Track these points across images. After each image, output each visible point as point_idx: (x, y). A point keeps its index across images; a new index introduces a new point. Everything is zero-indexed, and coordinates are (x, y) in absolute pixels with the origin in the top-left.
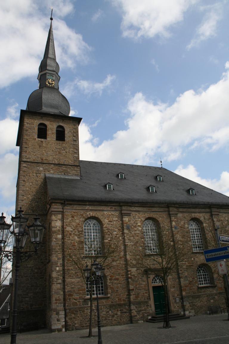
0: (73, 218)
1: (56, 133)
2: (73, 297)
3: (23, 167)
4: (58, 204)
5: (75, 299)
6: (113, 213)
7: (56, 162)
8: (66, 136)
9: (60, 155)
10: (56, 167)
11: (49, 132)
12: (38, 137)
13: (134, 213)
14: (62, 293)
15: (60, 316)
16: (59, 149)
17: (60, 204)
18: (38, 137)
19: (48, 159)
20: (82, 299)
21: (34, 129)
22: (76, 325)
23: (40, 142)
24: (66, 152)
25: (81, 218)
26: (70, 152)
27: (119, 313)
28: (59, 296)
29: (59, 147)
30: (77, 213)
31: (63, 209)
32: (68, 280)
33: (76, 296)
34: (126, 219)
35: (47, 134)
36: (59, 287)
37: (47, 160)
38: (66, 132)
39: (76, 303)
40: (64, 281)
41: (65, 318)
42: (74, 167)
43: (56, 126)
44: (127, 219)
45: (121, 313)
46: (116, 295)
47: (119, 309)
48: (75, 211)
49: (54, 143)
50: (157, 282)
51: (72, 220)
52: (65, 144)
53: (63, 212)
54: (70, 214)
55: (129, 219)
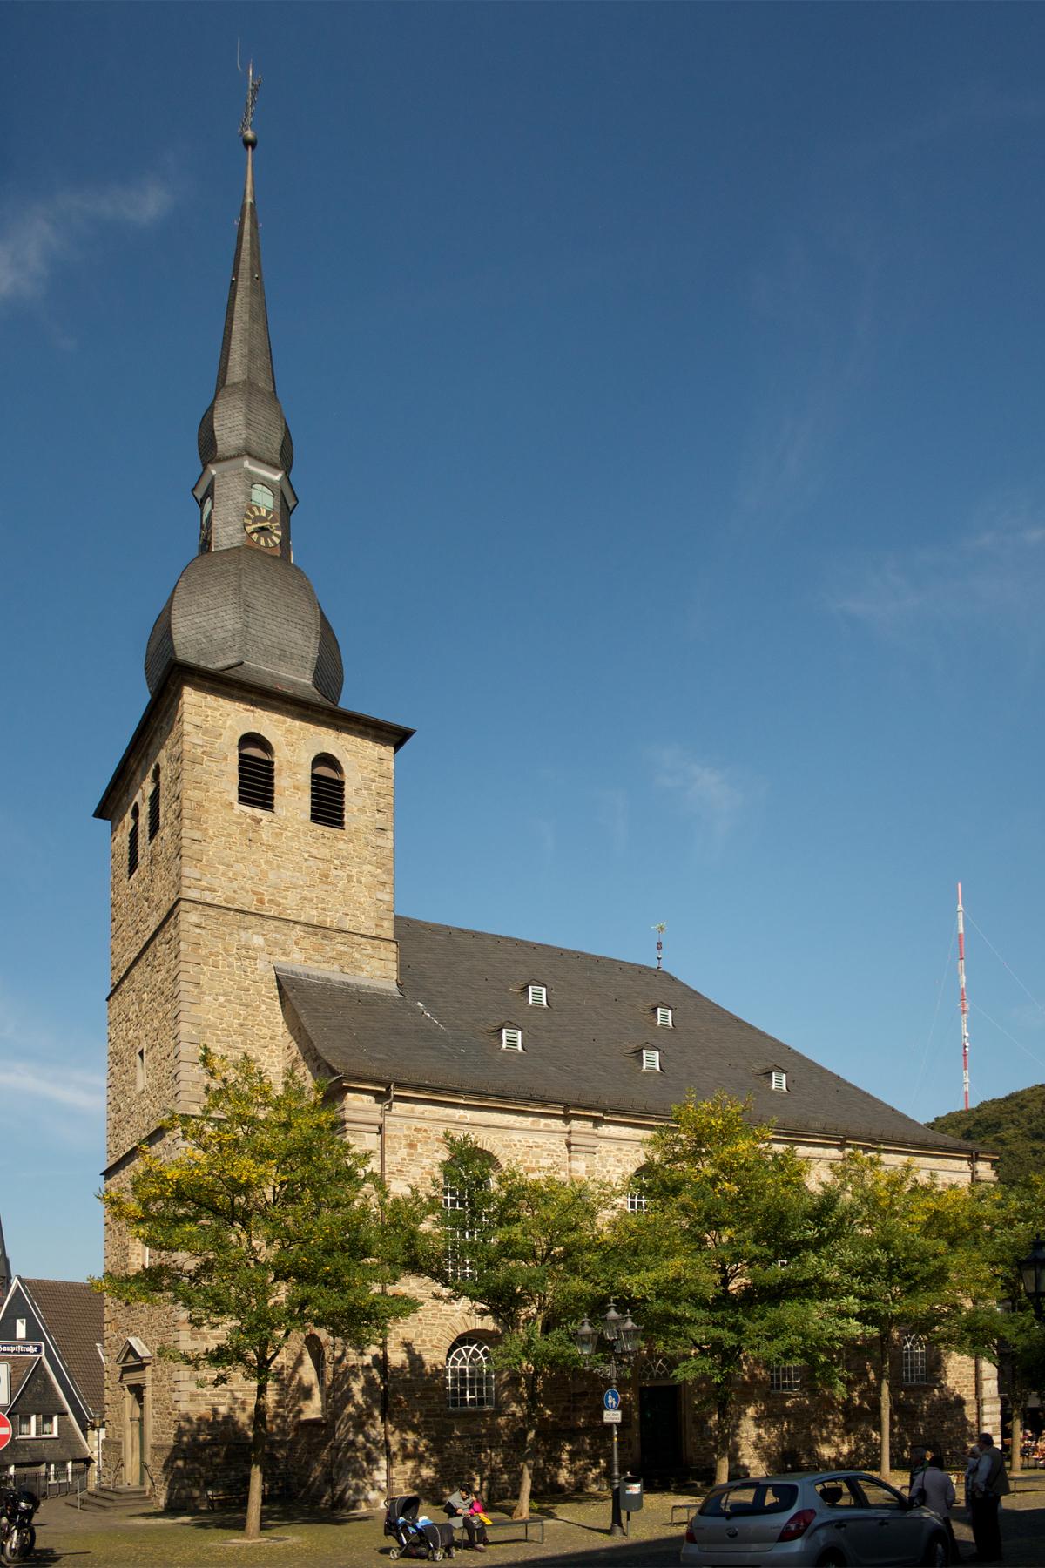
0: (412, 1151)
1: (313, 789)
3: (191, 924)
4: (365, 1097)
6: (540, 1139)
7: (309, 914)
8: (347, 805)
9: (325, 887)
10: (314, 938)
11: (281, 782)
12: (242, 800)
13: (604, 1145)
16: (322, 860)
17: (372, 1098)
18: (242, 800)
19: (282, 901)
21: (225, 759)
23: (249, 821)
24: (349, 877)
25: (437, 1151)
26: (363, 880)
29: (325, 853)
30: (425, 1131)
31: (382, 1114)
35: (276, 789)
37: (279, 905)
38: (349, 790)
42: (377, 942)
48: (419, 1127)
49: (305, 834)
51: (408, 1155)
52: (346, 842)
53: (381, 1127)
54: (405, 1136)
55: (587, 1167)
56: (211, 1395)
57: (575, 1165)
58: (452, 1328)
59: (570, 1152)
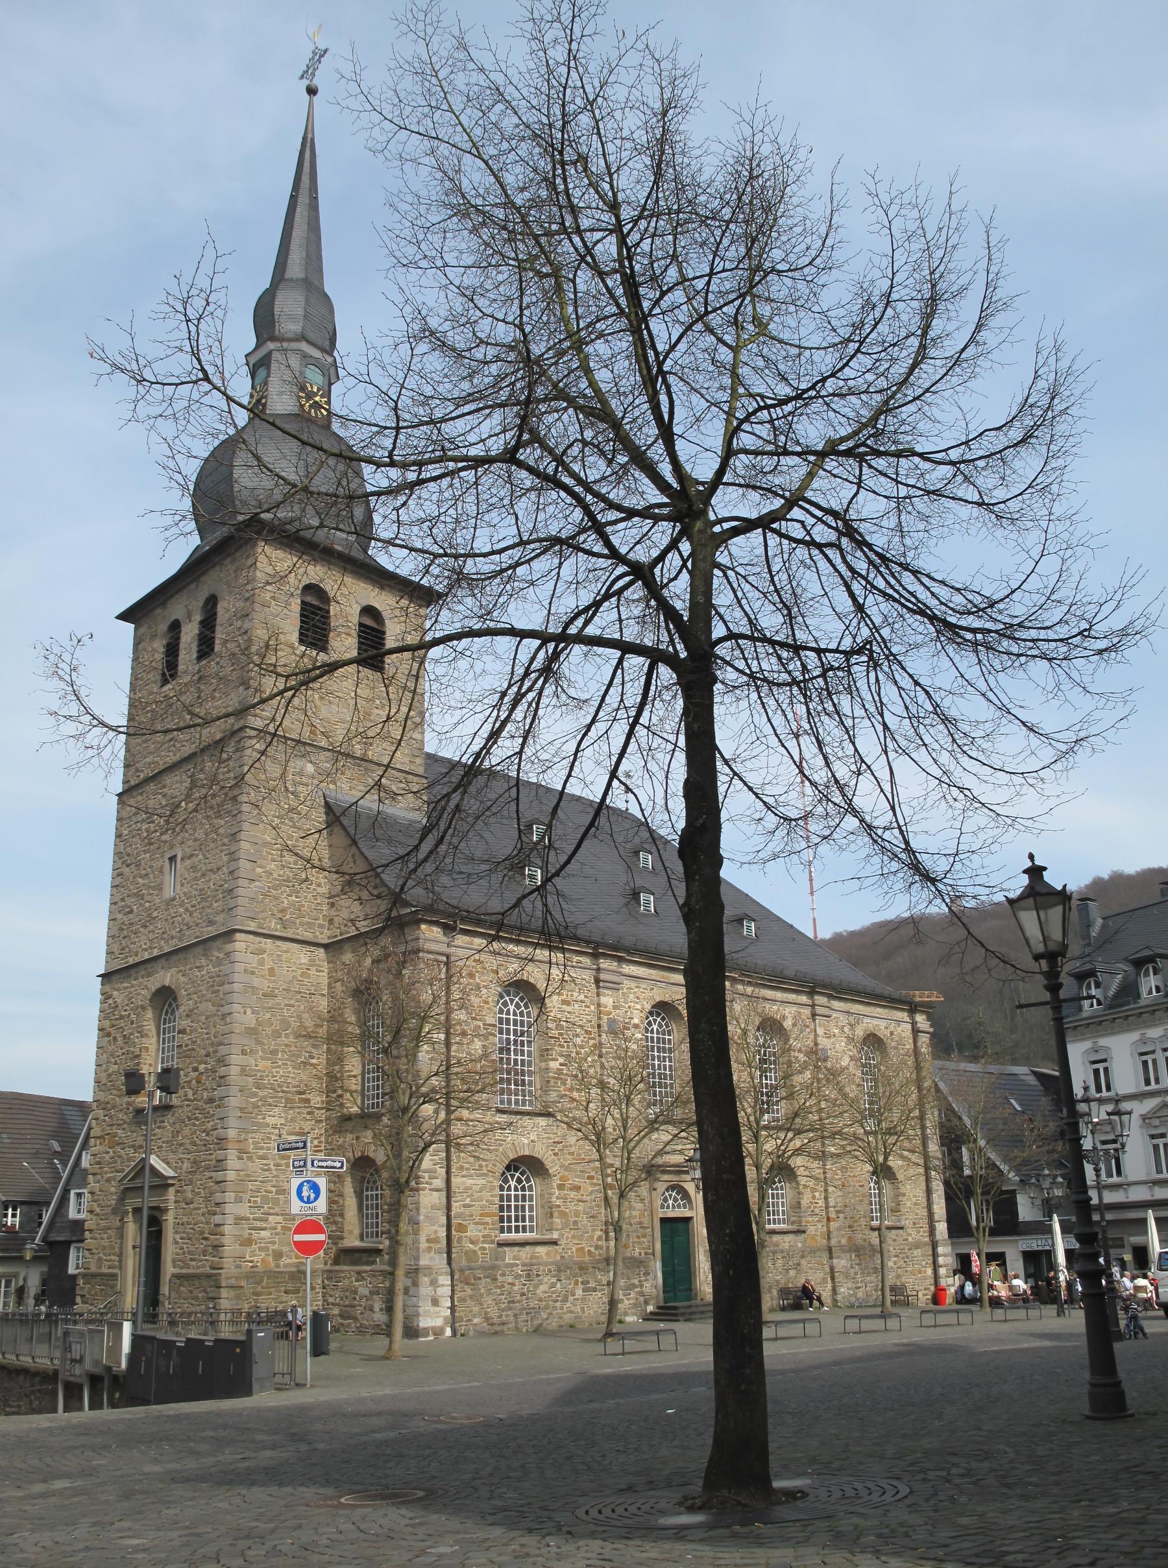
2: (469, 1234)
5: (472, 1242)
12: (301, 641)
13: (627, 983)
14: (444, 1220)
15: (440, 1291)
20: (492, 1242)
22: (476, 1321)
27: (579, 1292)
28: (435, 1228)
31: (449, 945)
32: (455, 1181)
33: (473, 1231)
34: (608, 1000)
36: (437, 1201)
39: (475, 1252)
40: (448, 1182)
41: (452, 1298)
43: (359, 608)
44: (611, 1000)
45: (584, 1290)
46: (573, 1237)
47: (580, 1279)
50: (668, 1207)
56: (254, 1219)
57: (603, 1000)
58: (504, 1153)
59: (598, 987)
